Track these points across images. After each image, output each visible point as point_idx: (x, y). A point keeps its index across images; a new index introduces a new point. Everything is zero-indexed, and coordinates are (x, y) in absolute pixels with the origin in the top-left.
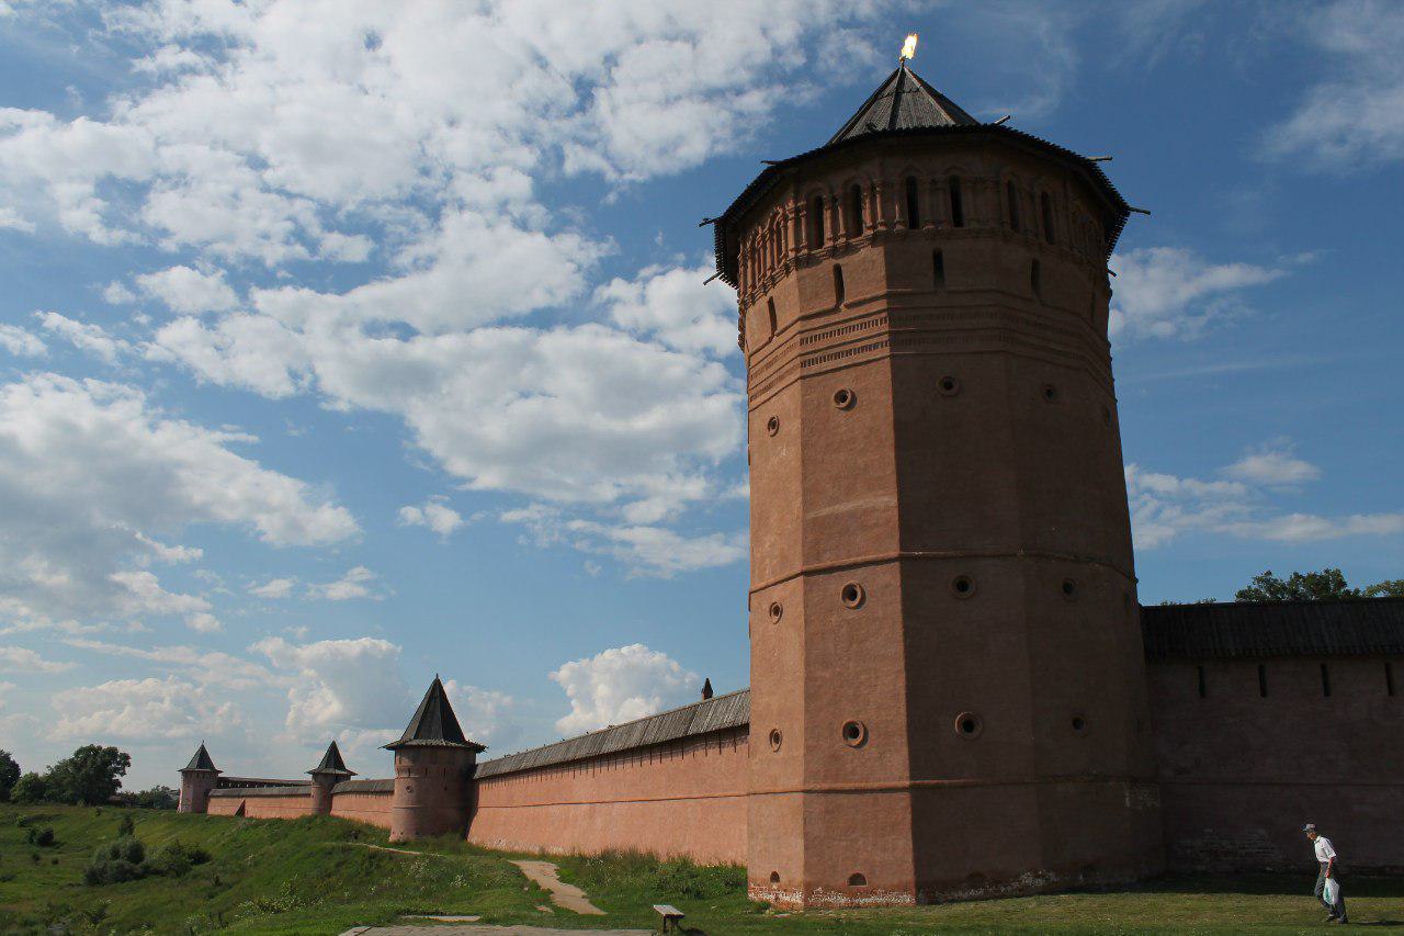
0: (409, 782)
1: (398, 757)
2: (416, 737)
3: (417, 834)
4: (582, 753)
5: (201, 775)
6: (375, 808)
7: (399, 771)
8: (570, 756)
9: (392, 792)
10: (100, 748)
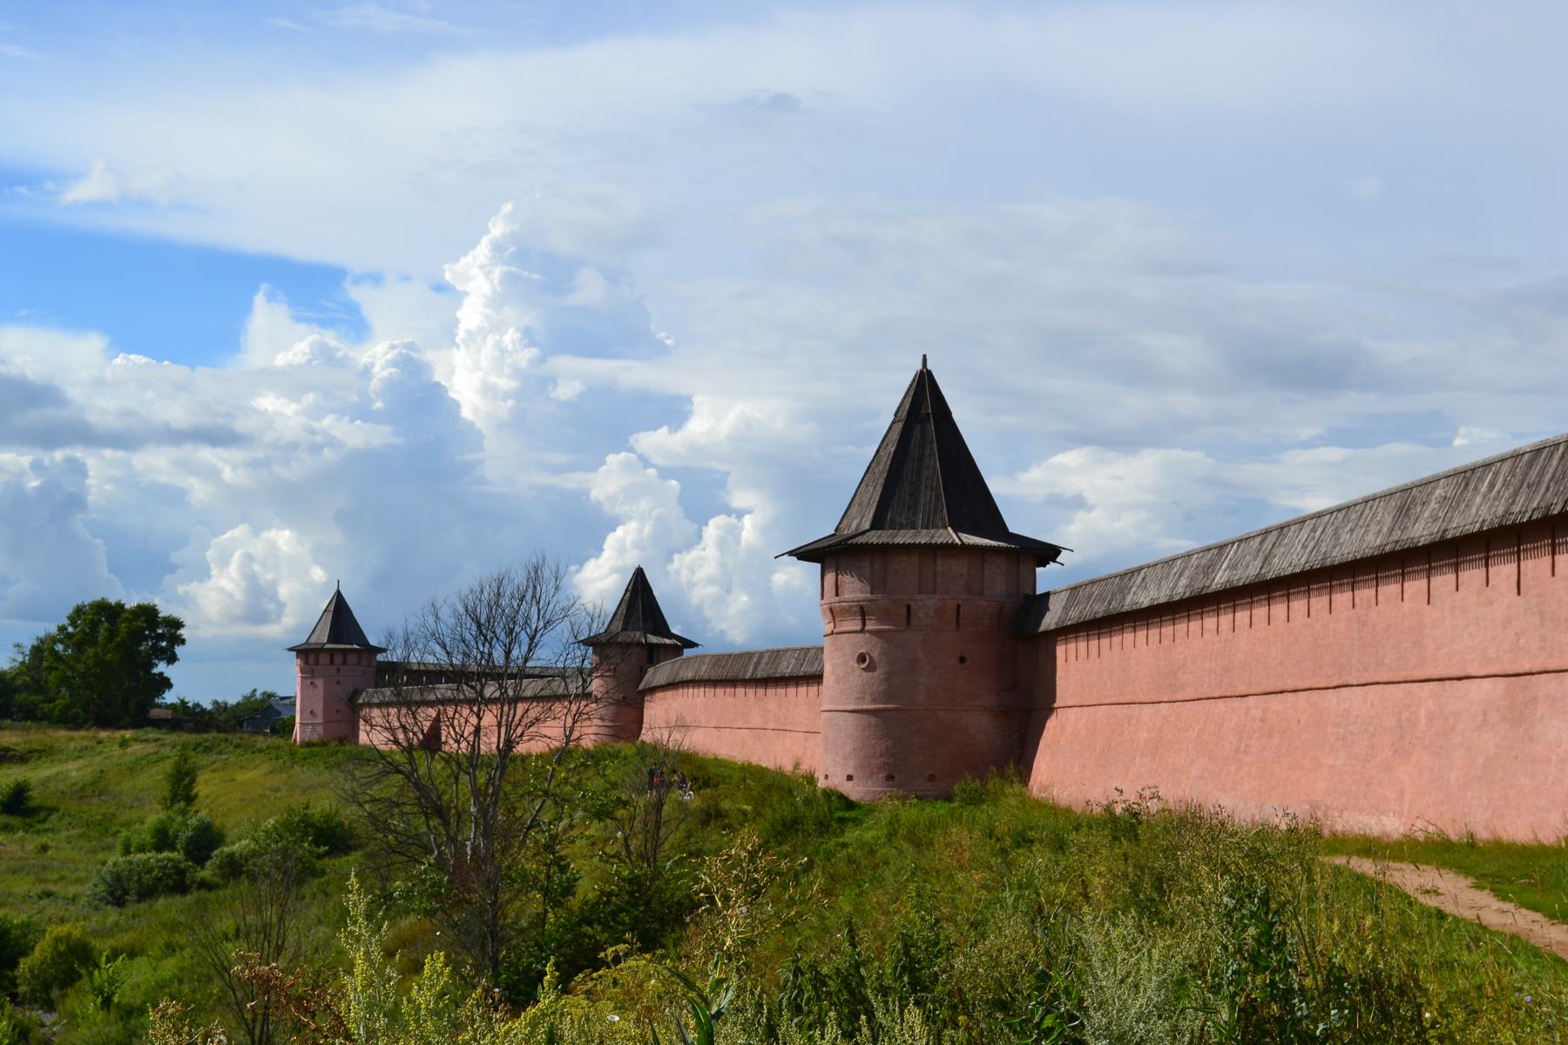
0: (862, 644)
1: (830, 577)
2: (877, 524)
3: (890, 777)
4: (1479, 513)
5: (338, 659)
6: (756, 721)
7: (834, 613)
8: (1421, 531)
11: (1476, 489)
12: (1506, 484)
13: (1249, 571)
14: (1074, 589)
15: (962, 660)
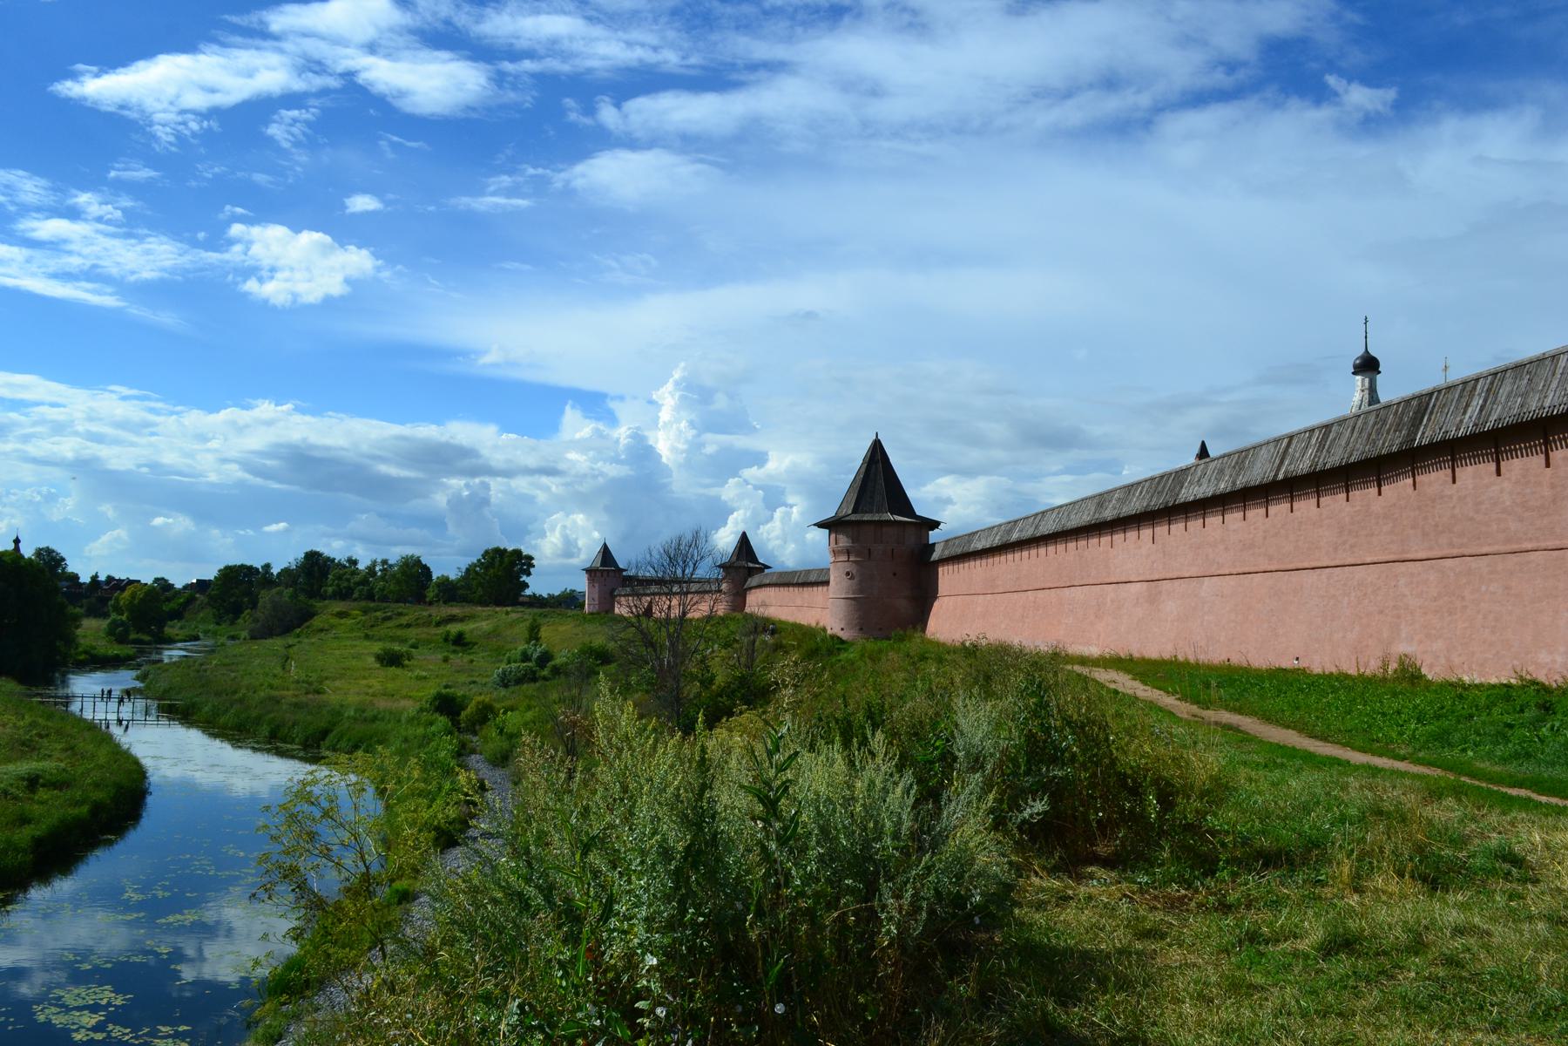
0: (848, 567)
1: (833, 536)
2: (855, 511)
3: (861, 629)
4: (1135, 505)
5: (605, 574)
6: (799, 602)
7: (835, 553)
8: (1108, 514)
9: (827, 583)
10: (505, 550)
11: (1134, 494)
12: (1147, 492)
13: (1029, 533)
14: (947, 541)
15: (895, 574)
